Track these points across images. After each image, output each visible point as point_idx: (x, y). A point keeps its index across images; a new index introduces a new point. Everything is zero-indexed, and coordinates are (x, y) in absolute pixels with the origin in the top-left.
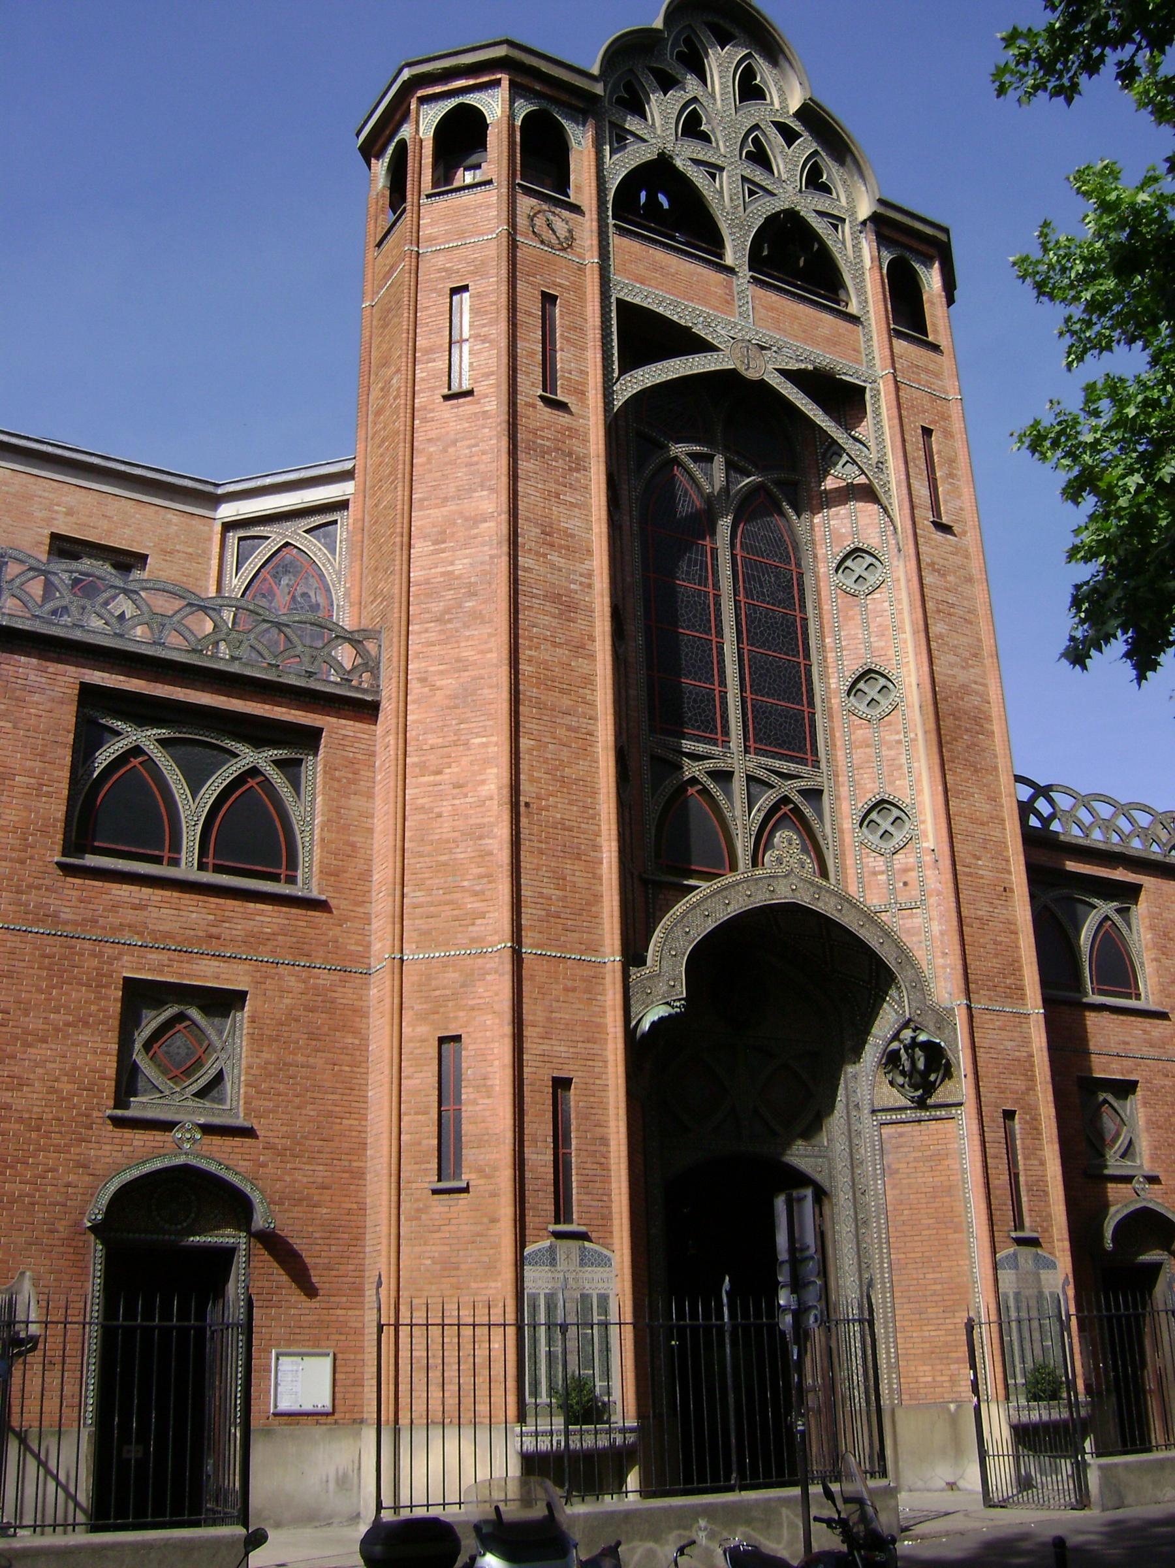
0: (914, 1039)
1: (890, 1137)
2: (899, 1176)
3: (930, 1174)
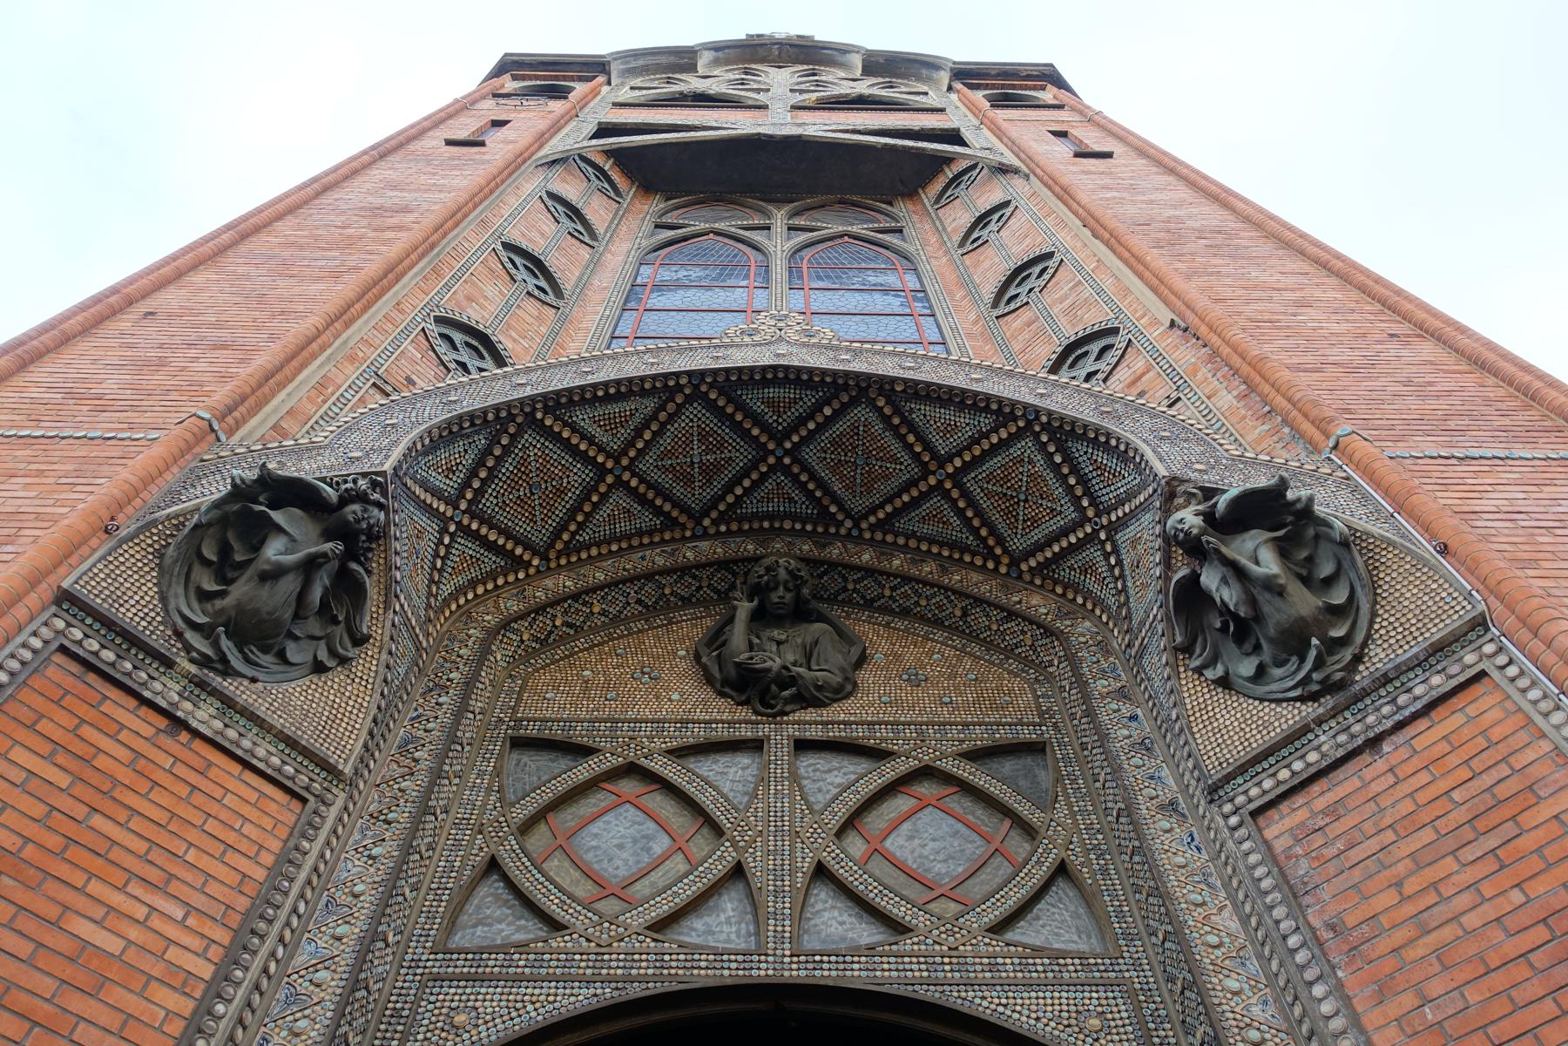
0: (1209, 517)
1: (1303, 834)
2: (1383, 945)
3: (1506, 877)
